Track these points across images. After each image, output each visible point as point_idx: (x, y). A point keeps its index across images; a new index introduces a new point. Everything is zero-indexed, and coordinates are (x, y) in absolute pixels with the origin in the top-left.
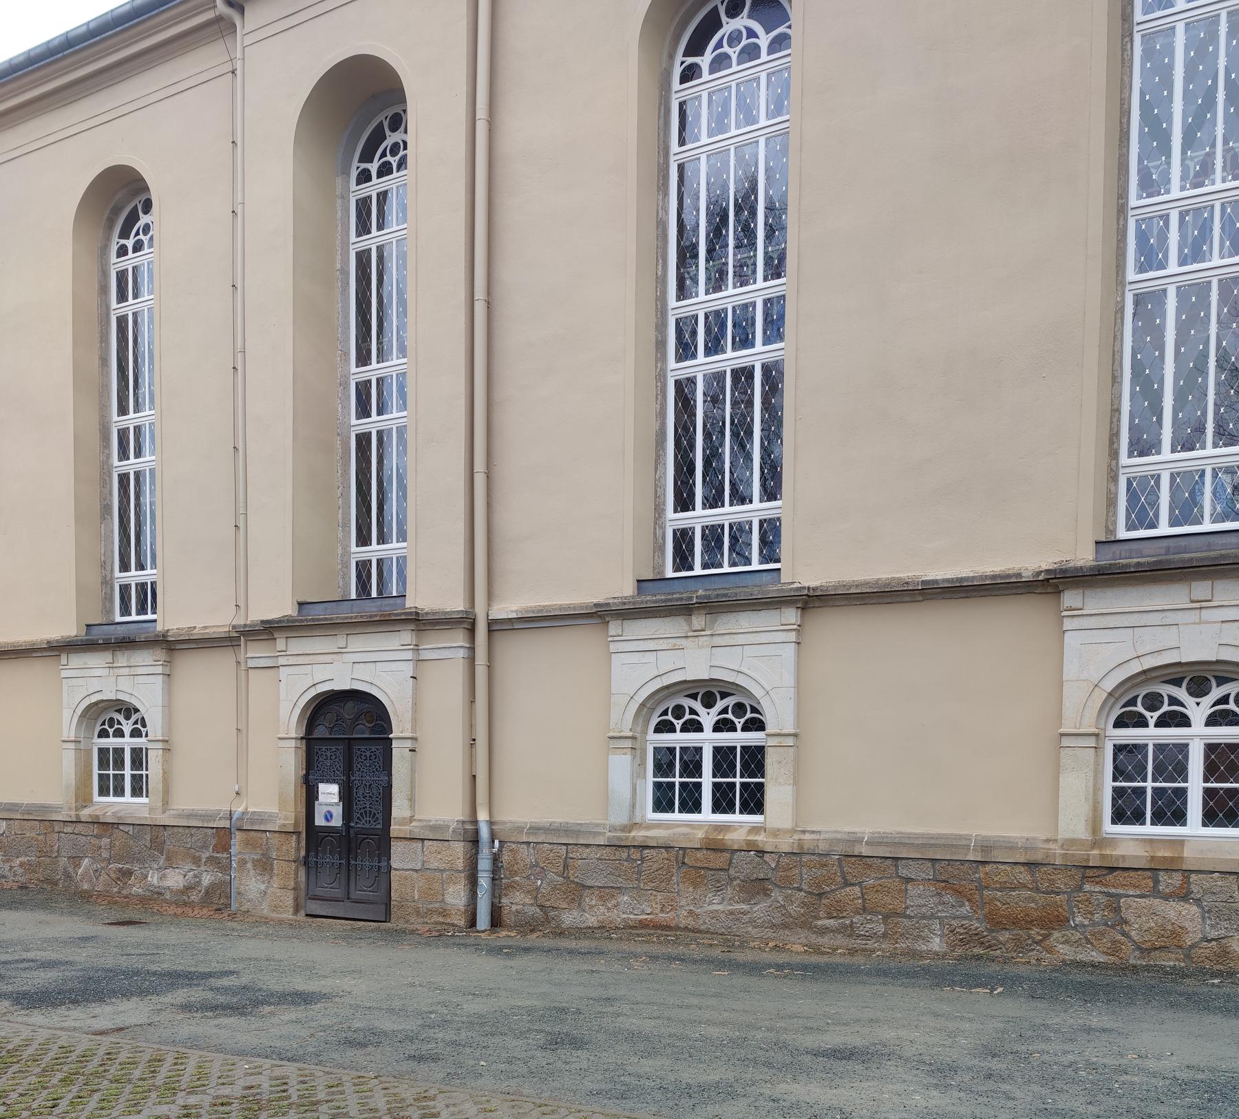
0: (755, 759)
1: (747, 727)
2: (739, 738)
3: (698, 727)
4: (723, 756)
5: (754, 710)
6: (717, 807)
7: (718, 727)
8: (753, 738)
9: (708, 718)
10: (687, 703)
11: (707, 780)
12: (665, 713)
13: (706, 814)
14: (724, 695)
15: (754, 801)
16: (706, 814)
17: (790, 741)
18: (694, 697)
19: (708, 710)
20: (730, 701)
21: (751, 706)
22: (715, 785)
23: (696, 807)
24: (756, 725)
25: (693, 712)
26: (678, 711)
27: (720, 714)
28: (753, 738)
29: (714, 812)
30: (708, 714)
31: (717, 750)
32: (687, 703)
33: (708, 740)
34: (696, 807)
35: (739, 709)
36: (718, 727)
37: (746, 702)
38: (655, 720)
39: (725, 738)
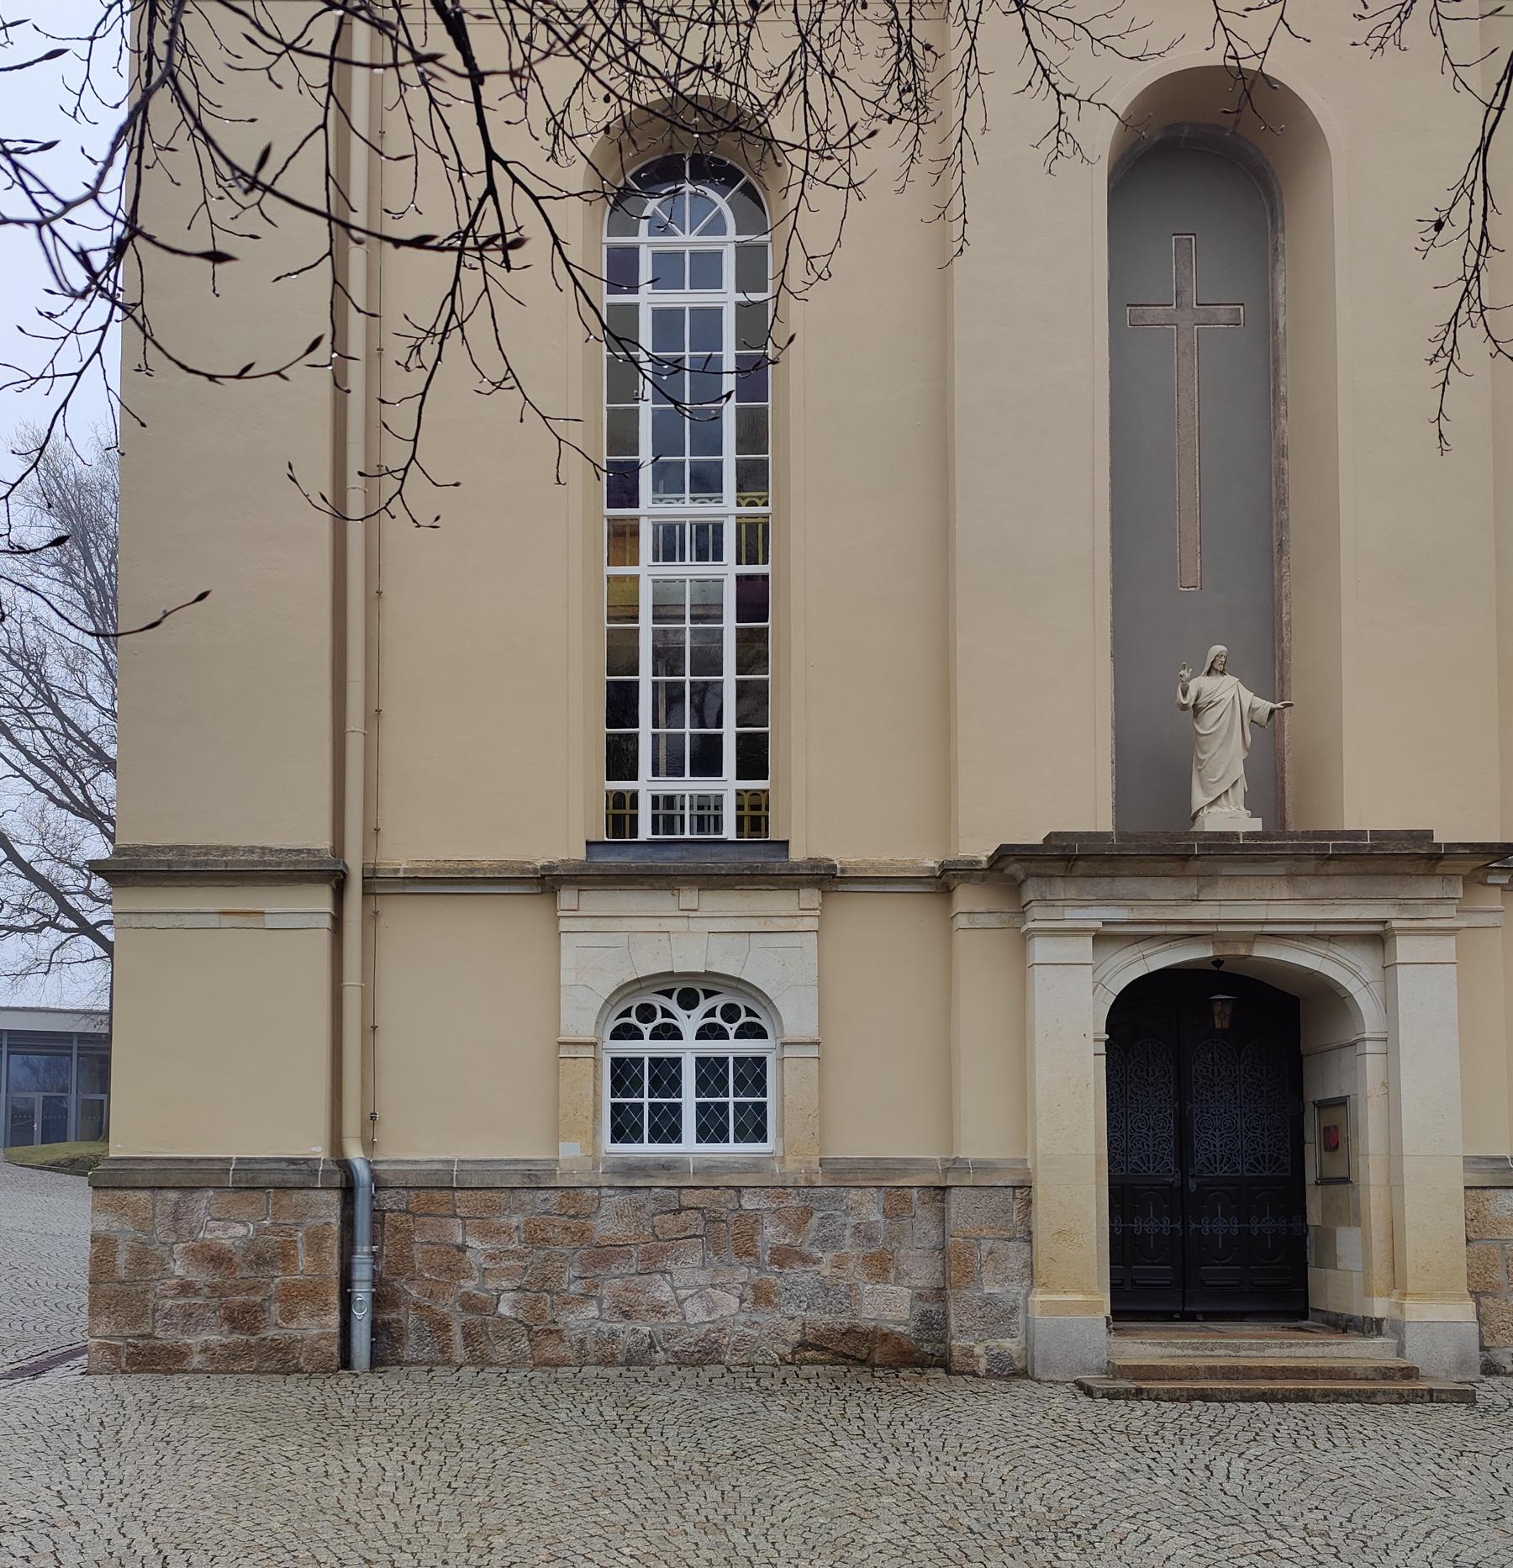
0: (753, 1073)
1: (744, 1033)
2: (733, 1047)
3: (676, 1034)
4: (711, 1073)
5: (750, 1013)
6: (703, 1135)
7: (705, 1033)
8: (750, 1047)
9: (689, 1022)
10: (659, 1002)
11: (689, 1100)
12: (627, 1013)
13: (689, 1146)
14: (709, 994)
15: (754, 1127)
16: (689, 1146)
17: (813, 1051)
18: (668, 994)
19: (689, 1012)
20: (718, 1002)
21: (746, 1008)
22: (699, 1105)
23: (675, 1135)
24: (758, 1032)
25: (666, 1013)
26: (646, 1013)
27: (706, 1016)
28: (750, 1047)
29: (698, 1141)
30: (689, 1017)
31: (701, 1062)
32: (659, 1002)
33: (689, 1049)
34: (674, 1134)
35: (730, 1012)
36: (705, 1033)
37: (741, 1003)
38: (613, 1024)
39: (713, 1047)
